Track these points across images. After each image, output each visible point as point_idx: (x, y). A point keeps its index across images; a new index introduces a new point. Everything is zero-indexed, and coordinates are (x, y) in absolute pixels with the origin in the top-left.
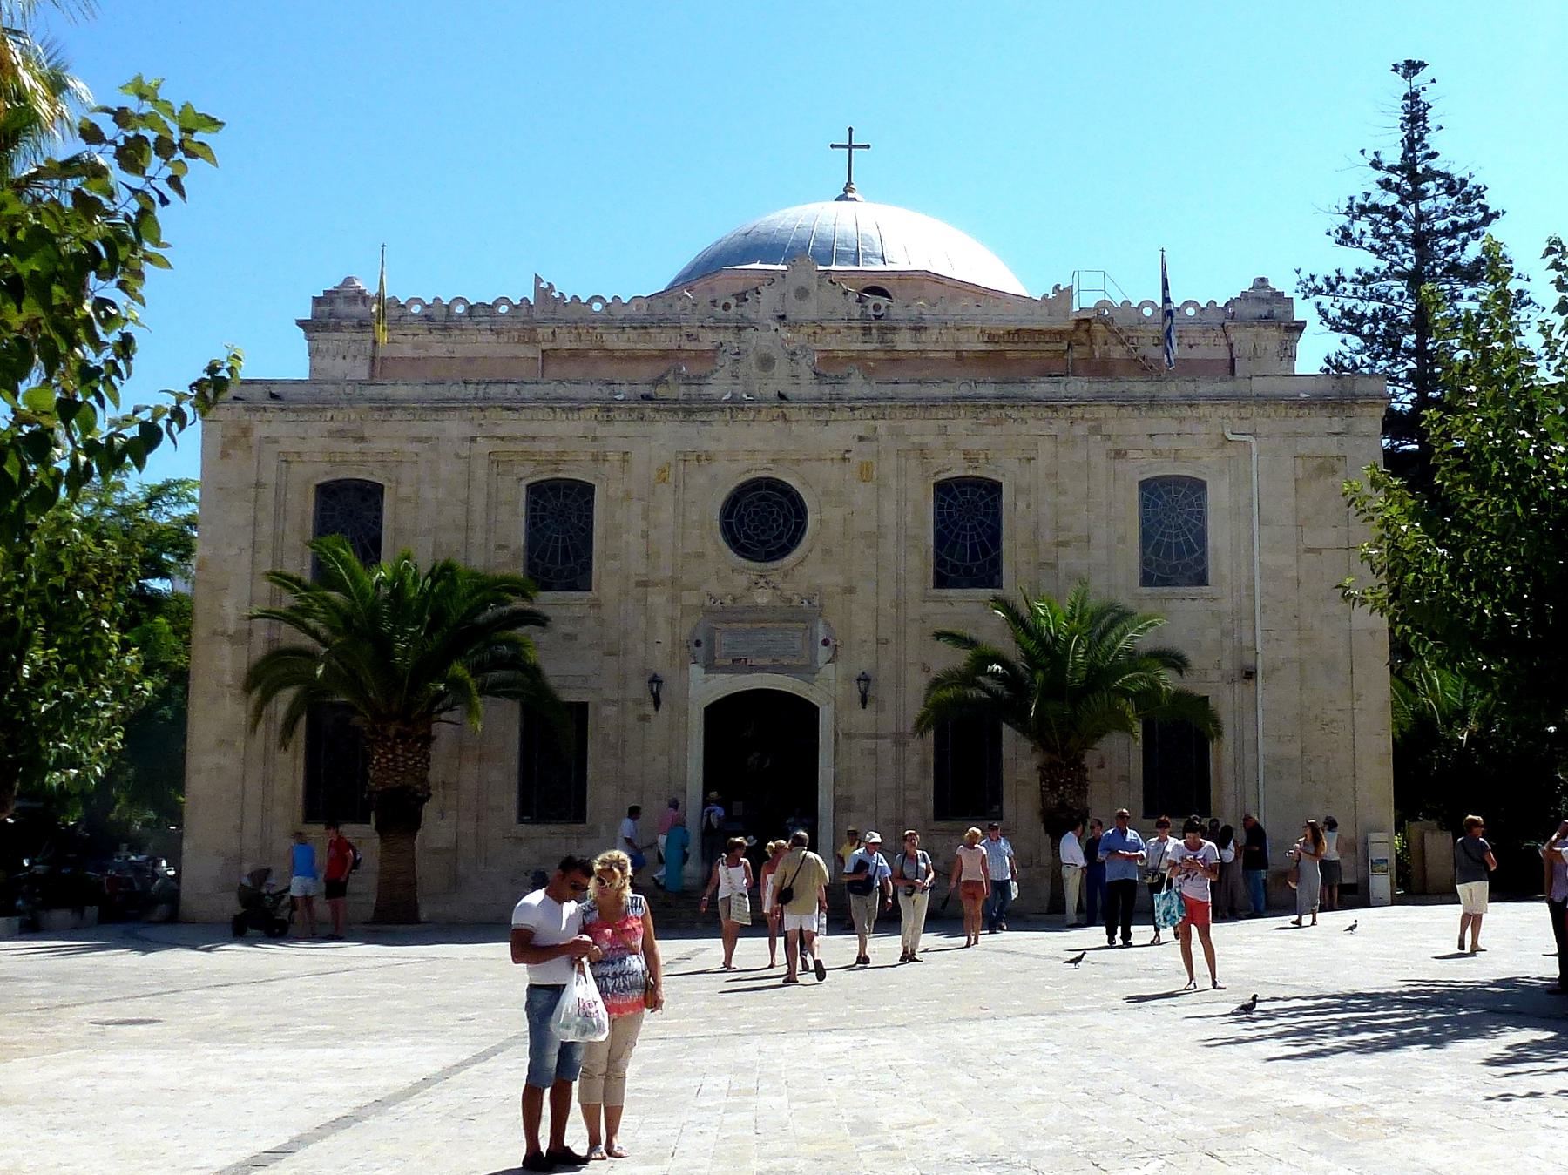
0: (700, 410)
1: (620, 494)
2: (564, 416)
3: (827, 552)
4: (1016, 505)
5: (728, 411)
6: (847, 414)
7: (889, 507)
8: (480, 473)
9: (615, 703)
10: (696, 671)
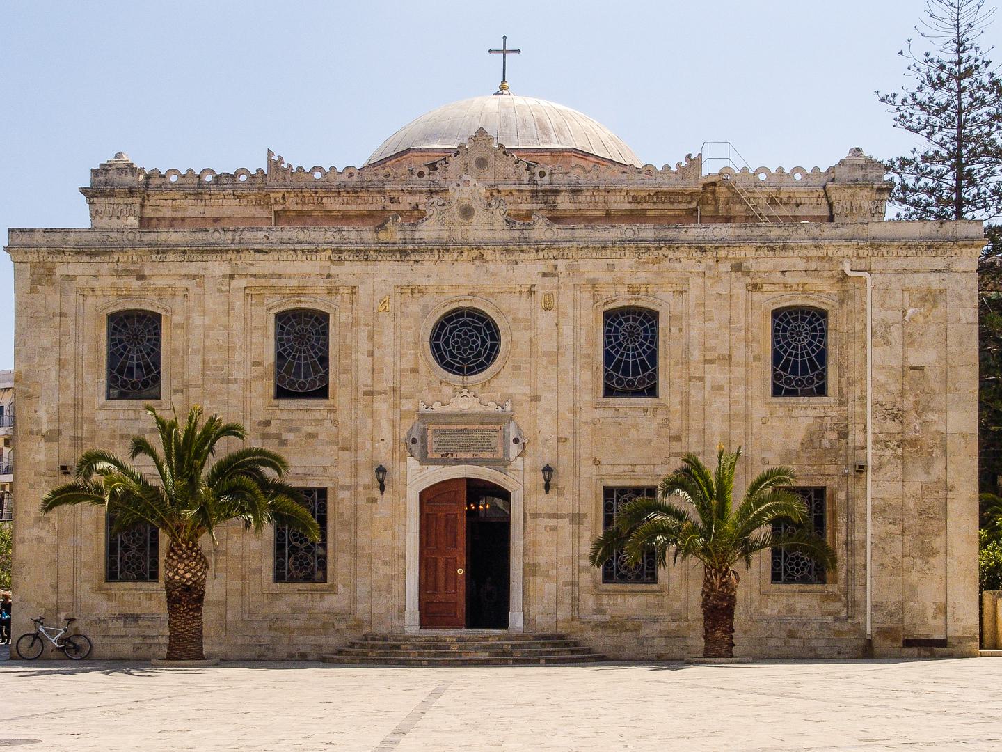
0: (413, 251)
1: (350, 321)
2: (304, 258)
3: (517, 368)
4: (670, 330)
5: (436, 252)
6: (533, 254)
7: (567, 330)
8: (238, 304)
9: (349, 488)
10: (412, 463)
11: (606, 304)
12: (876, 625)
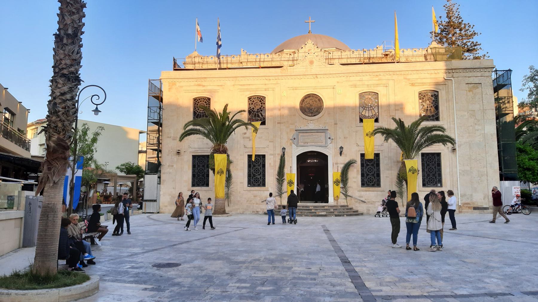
9: (273, 155)
11: (359, 91)
12: (462, 202)
